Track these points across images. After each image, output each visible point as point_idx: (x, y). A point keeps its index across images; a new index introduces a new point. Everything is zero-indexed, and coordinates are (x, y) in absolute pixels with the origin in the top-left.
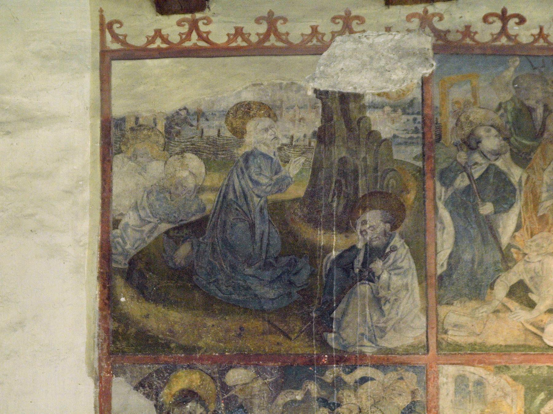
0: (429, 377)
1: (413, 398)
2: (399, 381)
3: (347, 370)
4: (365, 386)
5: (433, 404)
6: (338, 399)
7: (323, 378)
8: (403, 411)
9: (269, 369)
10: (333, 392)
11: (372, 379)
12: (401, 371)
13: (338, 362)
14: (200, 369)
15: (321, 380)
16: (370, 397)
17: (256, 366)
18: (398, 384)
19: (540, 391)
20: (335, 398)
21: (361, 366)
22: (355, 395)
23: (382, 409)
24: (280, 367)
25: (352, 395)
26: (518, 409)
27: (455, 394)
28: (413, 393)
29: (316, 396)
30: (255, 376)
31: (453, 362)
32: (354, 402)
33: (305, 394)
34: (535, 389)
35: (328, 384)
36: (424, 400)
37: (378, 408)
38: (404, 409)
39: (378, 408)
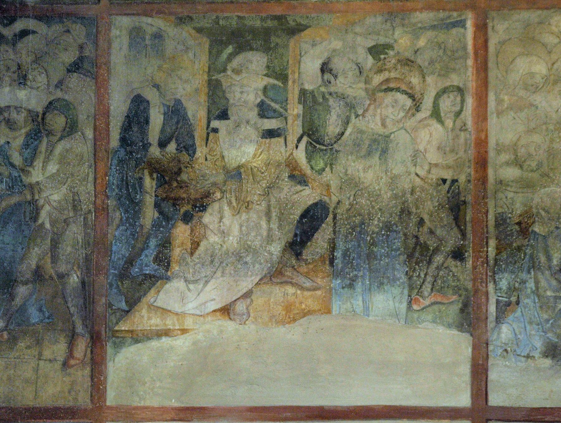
0: (100, 29)
4: (25, 40)
5: (103, 60)
11: (34, 32)
16: (32, 52)
18: (64, 37)
19: (226, 44)
22: (13, 49)
23: (45, 65)
25: (10, 51)
26: (202, 65)
28: (81, 47)
31: (127, 12)
32: (12, 57)
34: (221, 42)
37: (40, 65)
38: (70, 65)
39: (40, 65)
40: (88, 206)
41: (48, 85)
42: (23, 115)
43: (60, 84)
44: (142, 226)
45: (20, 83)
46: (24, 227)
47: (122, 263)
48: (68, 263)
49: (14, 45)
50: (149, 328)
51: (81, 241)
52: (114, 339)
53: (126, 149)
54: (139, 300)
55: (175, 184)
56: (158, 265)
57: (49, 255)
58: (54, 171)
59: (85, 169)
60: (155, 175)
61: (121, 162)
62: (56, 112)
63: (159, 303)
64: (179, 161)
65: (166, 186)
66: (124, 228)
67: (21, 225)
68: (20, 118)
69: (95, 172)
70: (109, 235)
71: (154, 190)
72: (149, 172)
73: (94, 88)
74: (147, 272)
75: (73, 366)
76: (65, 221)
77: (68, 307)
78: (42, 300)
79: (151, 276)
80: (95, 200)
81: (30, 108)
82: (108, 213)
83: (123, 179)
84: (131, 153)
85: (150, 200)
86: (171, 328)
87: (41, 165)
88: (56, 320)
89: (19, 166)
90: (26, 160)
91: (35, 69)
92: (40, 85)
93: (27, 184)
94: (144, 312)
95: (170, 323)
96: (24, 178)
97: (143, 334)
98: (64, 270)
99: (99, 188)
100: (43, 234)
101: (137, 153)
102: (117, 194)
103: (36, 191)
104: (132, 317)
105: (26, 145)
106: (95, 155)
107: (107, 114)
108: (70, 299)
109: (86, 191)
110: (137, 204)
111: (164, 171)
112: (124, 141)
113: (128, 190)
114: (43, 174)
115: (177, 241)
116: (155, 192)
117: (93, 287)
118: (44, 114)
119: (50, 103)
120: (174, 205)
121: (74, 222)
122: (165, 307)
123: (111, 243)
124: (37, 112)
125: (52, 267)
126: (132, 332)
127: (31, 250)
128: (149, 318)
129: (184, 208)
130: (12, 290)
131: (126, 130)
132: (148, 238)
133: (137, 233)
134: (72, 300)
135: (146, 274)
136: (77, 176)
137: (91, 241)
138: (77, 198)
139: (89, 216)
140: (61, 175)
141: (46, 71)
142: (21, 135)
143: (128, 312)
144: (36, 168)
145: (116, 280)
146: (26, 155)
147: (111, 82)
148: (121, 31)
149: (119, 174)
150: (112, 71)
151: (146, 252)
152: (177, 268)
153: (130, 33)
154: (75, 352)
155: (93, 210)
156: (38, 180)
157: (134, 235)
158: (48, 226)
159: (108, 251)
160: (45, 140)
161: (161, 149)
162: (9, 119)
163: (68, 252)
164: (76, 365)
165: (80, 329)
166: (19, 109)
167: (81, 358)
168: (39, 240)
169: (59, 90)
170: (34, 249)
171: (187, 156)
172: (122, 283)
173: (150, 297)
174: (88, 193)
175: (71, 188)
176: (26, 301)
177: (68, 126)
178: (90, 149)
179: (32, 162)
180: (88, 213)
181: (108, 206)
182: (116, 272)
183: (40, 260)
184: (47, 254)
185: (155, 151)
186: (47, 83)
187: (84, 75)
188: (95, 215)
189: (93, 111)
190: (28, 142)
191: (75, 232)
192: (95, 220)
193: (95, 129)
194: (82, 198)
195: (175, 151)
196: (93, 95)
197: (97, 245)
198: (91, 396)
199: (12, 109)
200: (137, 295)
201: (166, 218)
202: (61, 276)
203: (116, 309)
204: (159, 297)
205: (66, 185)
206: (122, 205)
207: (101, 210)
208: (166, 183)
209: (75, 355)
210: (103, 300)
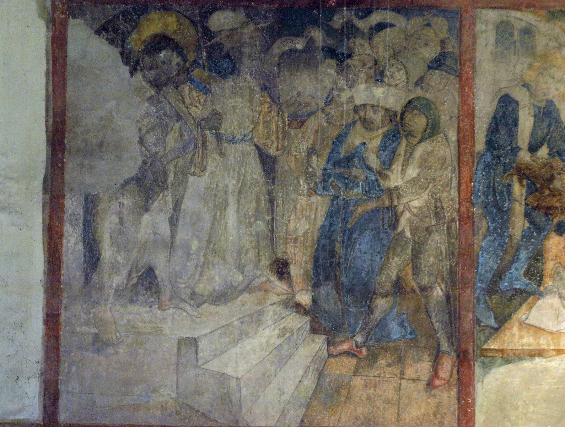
0: (464, 23)
1: (443, 48)
2: (426, 27)
3: (360, 14)
4: (382, 33)
6: (349, 48)
7: (329, 23)
8: (430, 64)
9: (263, 12)
10: (342, 41)
11: (392, 25)
12: (428, 16)
13: (349, 5)
14: (178, 12)
15: (328, 26)
16: (389, 46)
17: (246, 8)
18: (424, 32)
20: (345, 47)
21: (377, 9)
22: (370, 44)
23: (404, 61)
24: (277, 9)
25: (366, 45)
27: (496, 43)
28: (443, 42)
29: (321, 45)
30: (245, 19)
31: (493, 6)
32: (368, 52)
33: (308, 43)
35: (337, 30)
36: (456, 51)
38: (431, 61)
39: (398, 60)
40: (452, 214)
41: (408, 83)
42: (380, 114)
43: (420, 82)
44: (510, 237)
45: (377, 80)
46: (382, 235)
47: (489, 276)
48: (430, 274)
49: (370, 39)
50: (521, 348)
51: (444, 251)
52: (482, 358)
53: (492, 153)
54: (509, 316)
55: (547, 192)
56: (530, 279)
57: (410, 265)
58: (415, 175)
59: (448, 174)
60: (525, 182)
61: (487, 166)
62: (415, 112)
63: (531, 321)
64: (552, 167)
65: (537, 194)
66: (491, 238)
67: (379, 233)
68: (377, 118)
69: (459, 177)
70: (475, 246)
71: (524, 197)
72: (519, 178)
73: (457, 86)
74: (518, 287)
75: (437, 387)
76: (427, 229)
77: (431, 322)
78: (403, 314)
79: (521, 292)
80: (460, 207)
81: (388, 106)
82: (474, 222)
83: (490, 185)
84: (498, 157)
85: (519, 209)
86: (546, 348)
87: (400, 168)
88: (419, 336)
89: (376, 169)
90: (383, 163)
91: (393, 65)
92: (398, 82)
93: (384, 189)
94: (515, 330)
95: (544, 342)
96: (382, 182)
97: (514, 354)
98: (428, 282)
99: (463, 195)
100: (403, 243)
101: (505, 158)
102: (483, 202)
103: (395, 196)
104: (503, 335)
105: (384, 147)
106: (459, 158)
107: (472, 115)
108: (433, 314)
109: (450, 197)
110: (506, 212)
111: (535, 177)
112: (490, 144)
113: (494, 196)
114: (402, 179)
115: (551, 254)
116: (526, 199)
117: (459, 302)
118: (403, 114)
119: (410, 102)
120: (546, 214)
121: (437, 231)
122: (537, 325)
123: (478, 255)
124: (396, 112)
125: (414, 280)
126: (502, 351)
127: (391, 260)
128: (521, 337)
129: (558, 218)
130: (370, 302)
131: (492, 132)
132: (518, 250)
133: (506, 244)
134: (436, 315)
135: (516, 289)
136: (440, 181)
137: (456, 252)
138: (439, 205)
139: (453, 225)
140: (422, 180)
141: (405, 67)
142: (377, 136)
143: (497, 329)
144: (395, 172)
145: (483, 294)
146: (383, 157)
147: (477, 81)
148: (486, 26)
149: (485, 180)
150: (478, 68)
151: (516, 265)
152: (550, 283)
153: (497, 29)
154: (440, 371)
155: (457, 218)
156: (396, 184)
157: (502, 246)
158: (408, 234)
159: (474, 264)
160: (404, 142)
161: (531, 152)
162: (365, 119)
163: (431, 263)
164: (441, 385)
165: (445, 346)
166: (376, 108)
167: (447, 378)
168: (399, 250)
169: (419, 88)
170: (393, 259)
171: (560, 161)
172: (491, 298)
173: (521, 314)
174: (452, 200)
175: (433, 194)
176: (386, 315)
177: (429, 126)
178: (453, 152)
179: (390, 165)
180: (452, 221)
181: (473, 214)
182: (484, 286)
183: (400, 270)
184: (408, 265)
185: (524, 156)
186: (406, 81)
187: (446, 72)
188: (459, 224)
189: (457, 111)
190: (385, 144)
191: (438, 241)
192: (459, 229)
193: (458, 133)
194: (445, 206)
195: (547, 157)
196: (456, 94)
197: (463, 255)
198: (459, 419)
199: (368, 107)
200: (507, 311)
201: (537, 229)
202: (423, 289)
203: (484, 326)
204: (531, 314)
205: (428, 190)
206: (490, 213)
207: (466, 219)
208: (537, 190)
209: (440, 375)
210: (470, 316)
